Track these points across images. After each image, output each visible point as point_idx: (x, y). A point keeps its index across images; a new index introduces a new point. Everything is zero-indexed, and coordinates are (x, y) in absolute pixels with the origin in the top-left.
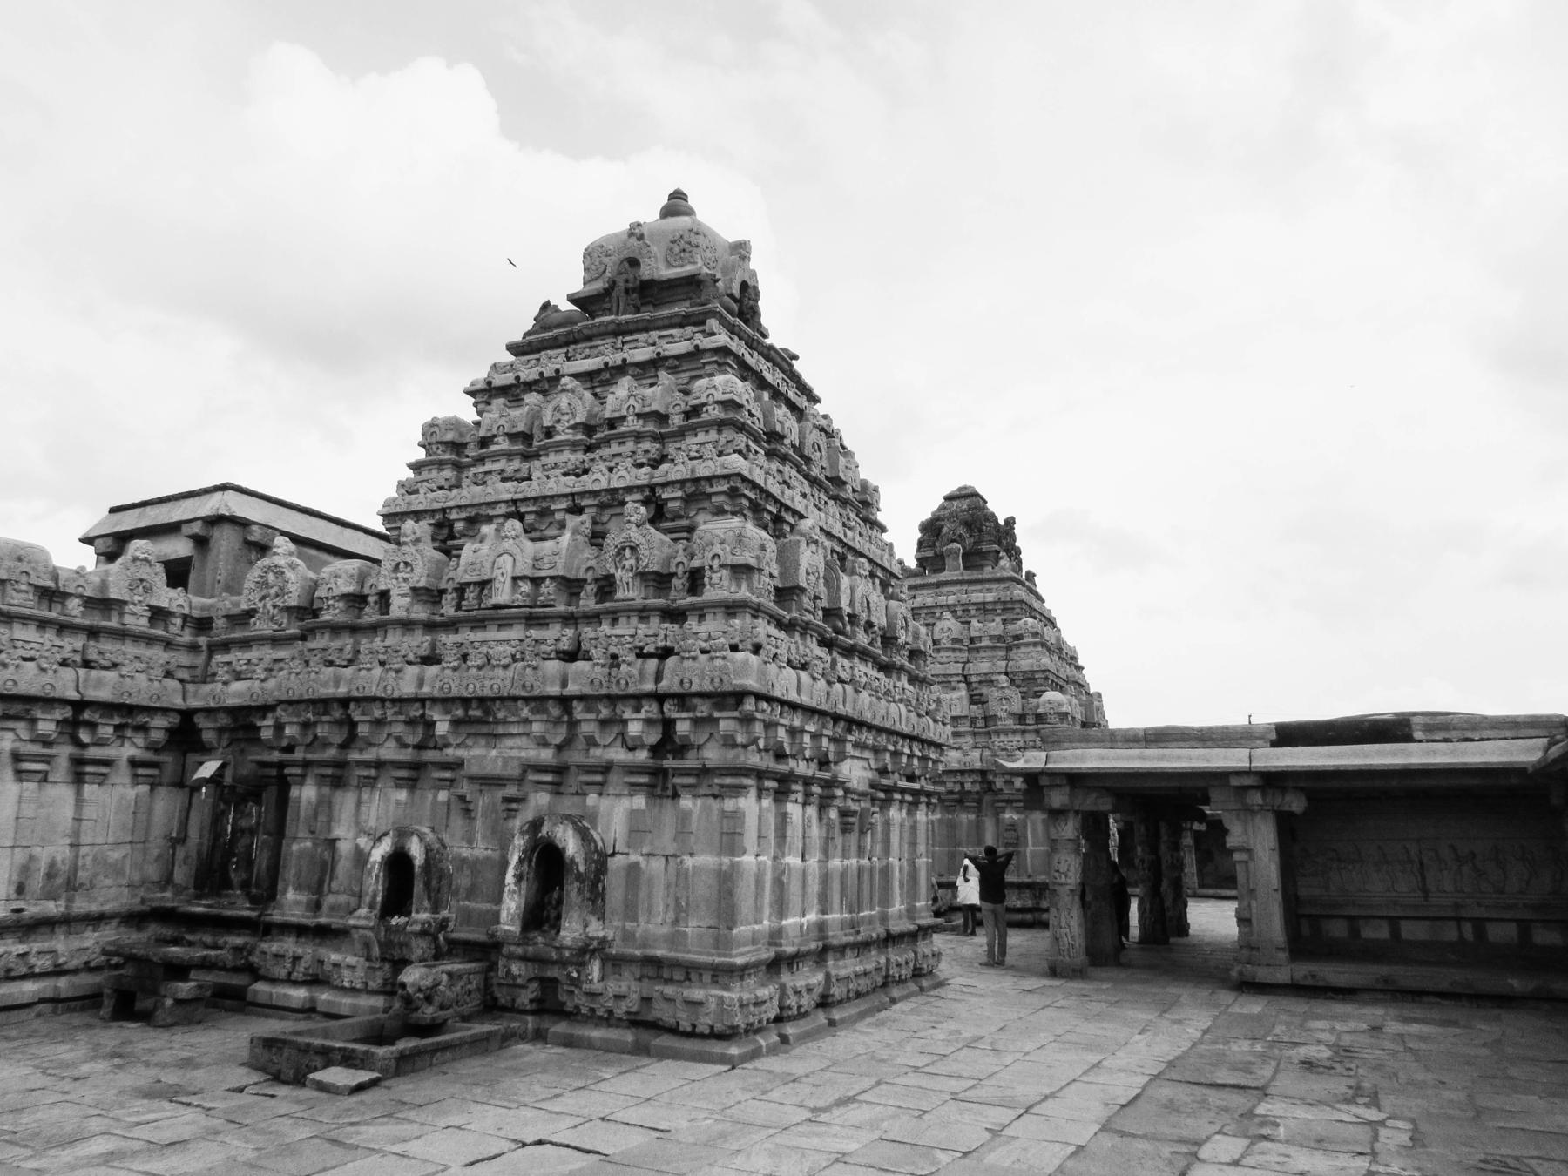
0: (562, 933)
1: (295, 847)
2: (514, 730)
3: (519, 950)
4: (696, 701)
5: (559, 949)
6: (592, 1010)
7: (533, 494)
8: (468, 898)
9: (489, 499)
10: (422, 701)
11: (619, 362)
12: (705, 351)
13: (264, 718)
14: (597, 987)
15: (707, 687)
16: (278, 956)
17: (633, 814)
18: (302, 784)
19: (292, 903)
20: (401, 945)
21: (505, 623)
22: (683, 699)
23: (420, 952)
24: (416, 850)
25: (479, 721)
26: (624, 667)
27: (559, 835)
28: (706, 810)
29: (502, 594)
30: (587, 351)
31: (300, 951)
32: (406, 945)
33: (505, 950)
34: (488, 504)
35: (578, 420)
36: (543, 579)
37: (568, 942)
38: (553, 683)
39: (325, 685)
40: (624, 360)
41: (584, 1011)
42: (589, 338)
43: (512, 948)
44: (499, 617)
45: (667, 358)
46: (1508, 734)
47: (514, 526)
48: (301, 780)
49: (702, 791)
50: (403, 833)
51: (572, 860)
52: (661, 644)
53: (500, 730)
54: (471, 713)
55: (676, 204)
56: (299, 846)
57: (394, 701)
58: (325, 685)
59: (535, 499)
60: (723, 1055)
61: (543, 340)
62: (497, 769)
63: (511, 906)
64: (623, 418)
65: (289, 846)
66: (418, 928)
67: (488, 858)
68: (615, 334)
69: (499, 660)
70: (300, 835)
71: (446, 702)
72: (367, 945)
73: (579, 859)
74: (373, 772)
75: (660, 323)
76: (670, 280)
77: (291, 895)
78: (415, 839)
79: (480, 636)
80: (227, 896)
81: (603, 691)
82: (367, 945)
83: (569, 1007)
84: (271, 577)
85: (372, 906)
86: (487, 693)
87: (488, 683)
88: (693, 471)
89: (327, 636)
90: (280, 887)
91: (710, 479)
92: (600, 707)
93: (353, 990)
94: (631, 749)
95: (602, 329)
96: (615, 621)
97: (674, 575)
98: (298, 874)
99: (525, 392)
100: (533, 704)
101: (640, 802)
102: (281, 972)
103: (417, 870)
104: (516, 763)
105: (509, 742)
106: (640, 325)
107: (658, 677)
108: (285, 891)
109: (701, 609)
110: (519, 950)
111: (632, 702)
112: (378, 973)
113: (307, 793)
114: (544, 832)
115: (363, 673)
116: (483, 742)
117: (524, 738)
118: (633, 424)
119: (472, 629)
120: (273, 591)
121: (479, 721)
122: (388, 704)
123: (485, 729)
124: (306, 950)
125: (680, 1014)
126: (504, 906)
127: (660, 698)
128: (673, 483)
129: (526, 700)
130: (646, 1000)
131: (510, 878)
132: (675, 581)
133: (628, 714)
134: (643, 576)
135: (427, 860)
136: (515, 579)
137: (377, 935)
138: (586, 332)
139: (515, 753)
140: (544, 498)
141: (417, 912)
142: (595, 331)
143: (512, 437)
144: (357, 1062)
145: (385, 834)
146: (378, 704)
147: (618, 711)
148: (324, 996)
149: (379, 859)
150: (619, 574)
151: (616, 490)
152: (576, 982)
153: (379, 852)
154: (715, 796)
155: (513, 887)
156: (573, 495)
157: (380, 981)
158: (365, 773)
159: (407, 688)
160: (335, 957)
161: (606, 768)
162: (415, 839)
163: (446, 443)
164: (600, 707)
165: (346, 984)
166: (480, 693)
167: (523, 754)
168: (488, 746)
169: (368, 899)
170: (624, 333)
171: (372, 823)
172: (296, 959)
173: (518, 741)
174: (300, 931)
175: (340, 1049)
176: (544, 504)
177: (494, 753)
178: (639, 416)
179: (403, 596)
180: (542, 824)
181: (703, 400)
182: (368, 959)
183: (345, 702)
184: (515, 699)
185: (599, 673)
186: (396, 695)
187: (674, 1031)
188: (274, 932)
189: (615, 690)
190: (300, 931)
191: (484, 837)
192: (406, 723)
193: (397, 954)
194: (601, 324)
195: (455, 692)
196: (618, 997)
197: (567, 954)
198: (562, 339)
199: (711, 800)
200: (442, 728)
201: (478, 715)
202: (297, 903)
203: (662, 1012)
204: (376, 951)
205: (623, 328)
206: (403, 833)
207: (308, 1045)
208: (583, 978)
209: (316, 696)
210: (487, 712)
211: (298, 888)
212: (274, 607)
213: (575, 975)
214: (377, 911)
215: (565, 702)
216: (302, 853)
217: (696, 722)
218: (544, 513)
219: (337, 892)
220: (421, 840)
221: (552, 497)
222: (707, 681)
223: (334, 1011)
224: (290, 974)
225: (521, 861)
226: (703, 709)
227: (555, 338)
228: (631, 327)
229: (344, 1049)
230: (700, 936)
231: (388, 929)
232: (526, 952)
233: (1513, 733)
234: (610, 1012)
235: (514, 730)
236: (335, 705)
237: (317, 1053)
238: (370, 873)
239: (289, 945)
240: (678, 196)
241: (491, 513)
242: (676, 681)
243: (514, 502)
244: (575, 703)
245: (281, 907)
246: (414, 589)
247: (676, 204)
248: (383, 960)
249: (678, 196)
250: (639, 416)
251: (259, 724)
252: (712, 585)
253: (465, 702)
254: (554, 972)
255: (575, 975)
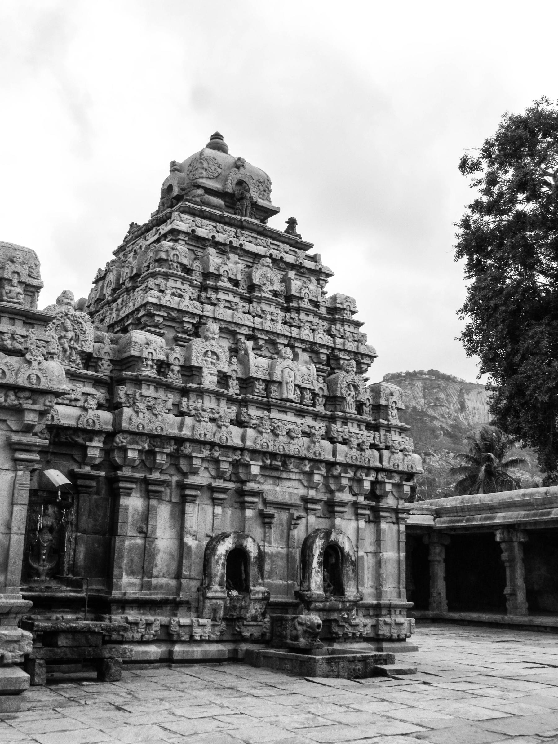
0: (347, 593)
1: (127, 543)
2: (293, 476)
3: (321, 605)
4: (395, 475)
5: (343, 602)
6: (354, 634)
7: (268, 329)
8: (269, 578)
9: (240, 322)
10: (242, 450)
11: (279, 258)
12: (324, 273)
13: (91, 440)
14: (357, 621)
15: (406, 469)
16: (136, 624)
17: (358, 529)
18: (128, 495)
19: (128, 584)
20: (241, 608)
21: (284, 410)
22: (389, 472)
23: (253, 611)
24: (251, 547)
25: (276, 469)
26: (366, 451)
27: (340, 540)
28: (391, 530)
29: (291, 396)
30: (251, 239)
31: (152, 618)
32: (246, 608)
33: (313, 606)
34: (236, 324)
35: (275, 289)
36: (306, 389)
37: (352, 598)
38: (329, 454)
39: (171, 426)
40: (282, 258)
41: (350, 635)
42: (243, 228)
43: (317, 604)
44: (284, 406)
45: (304, 267)
46: (420, 513)
47: (304, 356)
48: (128, 492)
49: (389, 520)
50: (241, 535)
51: (348, 554)
52: (372, 442)
53: (284, 475)
54: (275, 463)
55: (217, 143)
56: (129, 541)
57: (221, 446)
58: (171, 426)
59: (267, 332)
60: (404, 648)
61: (210, 213)
62: (286, 499)
63: (317, 580)
64: (301, 298)
65: (123, 541)
66: (260, 596)
67: (279, 553)
68: (259, 233)
69: (289, 433)
70: (130, 534)
71: (254, 453)
72: (215, 610)
73: (351, 553)
74: (199, 493)
75: (283, 239)
76: (262, 207)
77: (125, 579)
78: (250, 540)
79: (282, 416)
80: (35, 581)
81: (358, 463)
82: (215, 610)
83: (340, 633)
84: (69, 324)
85: (220, 584)
86: (291, 453)
87: (292, 447)
88: (357, 348)
89: (152, 388)
90: (116, 572)
91: (362, 355)
92: (349, 471)
93: (202, 641)
94: (354, 495)
95: (255, 227)
96: (345, 423)
97: (365, 404)
98: (131, 561)
99: (211, 246)
100: (312, 464)
101: (362, 524)
102: (138, 636)
103: (252, 560)
104: (296, 497)
105: (287, 483)
106: (274, 235)
107: (381, 461)
108: (121, 577)
109: (390, 428)
110: (321, 605)
111: (366, 471)
112: (216, 629)
113: (133, 503)
114: (332, 537)
115: (203, 424)
116: (271, 481)
117: (297, 482)
118: (305, 304)
119: (296, 415)
120: (70, 334)
121: (276, 469)
122: (217, 448)
123: (275, 474)
124: (159, 619)
125: (393, 631)
126: (312, 580)
127: (378, 470)
128: (345, 350)
129: (310, 460)
130: (375, 627)
131: (315, 564)
132: (367, 409)
133: (364, 478)
134: (356, 401)
135: (258, 553)
136: (295, 385)
137: (225, 602)
138: (244, 223)
139: (291, 490)
140: (273, 333)
141: (254, 586)
142: (251, 226)
143: (230, 280)
144: (382, 661)
145: (228, 536)
146: (208, 447)
147: (358, 475)
148: (177, 648)
149: (224, 553)
150: (349, 399)
151: (315, 344)
152: (347, 620)
153: (223, 548)
154: (394, 523)
155: (317, 569)
156: (291, 337)
157: (218, 634)
158: (194, 493)
159: (237, 441)
160: (184, 621)
161: (343, 504)
162: (250, 540)
163: (181, 264)
164: (349, 471)
165: (198, 638)
166: (287, 452)
167: (296, 491)
168: (274, 484)
169: (218, 579)
170: (274, 239)
171: (194, 528)
172: (149, 624)
173: (291, 484)
174: (142, 604)
175: (372, 656)
176: (272, 337)
177: (278, 489)
178: (310, 301)
179: (214, 375)
180: (331, 534)
181: (345, 307)
182: (214, 619)
183: (180, 441)
184: (302, 459)
185: (355, 452)
186: (230, 443)
187: (391, 640)
188: (114, 608)
189: (363, 464)
190: (142, 604)
191: (276, 540)
192: (230, 463)
193: (235, 614)
194: (257, 225)
195: (271, 449)
196: (365, 626)
197: (348, 604)
198: (227, 220)
199: (392, 525)
200: (255, 470)
201: (277, 464)
202: (131, 585)
203: (384, 631)
204: (221, 613)
205: (265, 232)
206: (241, 535)
207: (354, 657)
208: (350, 618)
209: (164, 433)
210: (284, 464)
211: (132, 573)
212: (70, 347)
213: (346, 616)
214: (225, 588)
215: (330, 465)
216: (132, 548)
217: (393, 484)
218: (274, 343)
219: (157, 577)
220: (254, 541)
221: (278, 334)
222: (405, 466)
223: (189, 657)
224: (143, 636)
225: (321, 554)
226: (397, 479)
227: (222, 217)
228: (269, 234)
229: (375, 656)
230: (391, 592)
231: (232, 598)
232: (325, 605)
233: (420, 513)
234: (361, 634)
235: (293, 476)
236: (173, 442)
237: (359, 661)
238: (217, 562)
239: (132, 615)
240: (217, 136)
241: (238, 331)
242: (392, 464)
243: (254, 329)
244: (338, 467)
245: (119, 587)
246: (219, 372)
247: (217, 143)
248: (224, 619)
249: (217, 136)
250: (310, 301)
251: (88, 444)
252: (393, 416)
253: (273, 455)
254: (335, 616)
255: (346, 616)
